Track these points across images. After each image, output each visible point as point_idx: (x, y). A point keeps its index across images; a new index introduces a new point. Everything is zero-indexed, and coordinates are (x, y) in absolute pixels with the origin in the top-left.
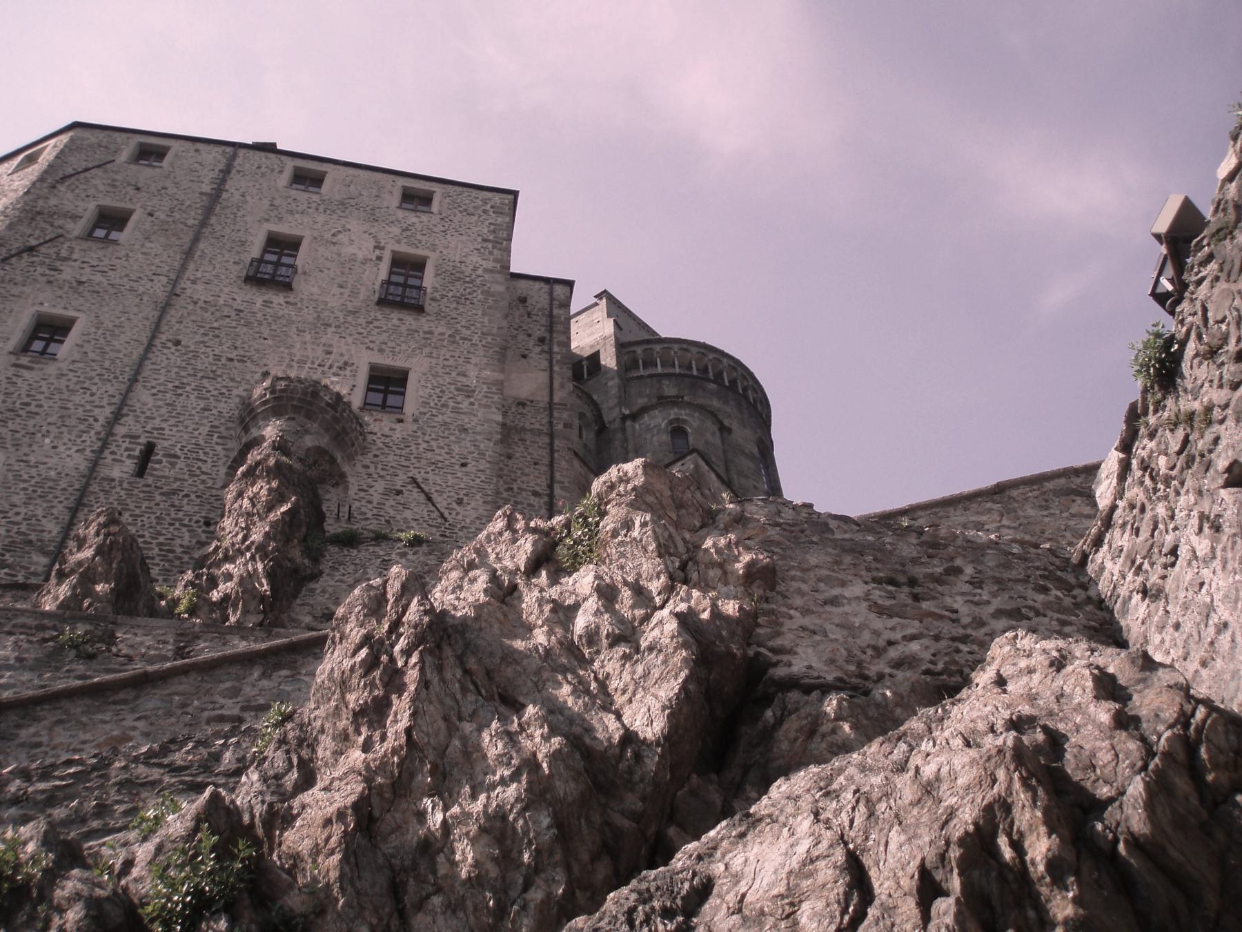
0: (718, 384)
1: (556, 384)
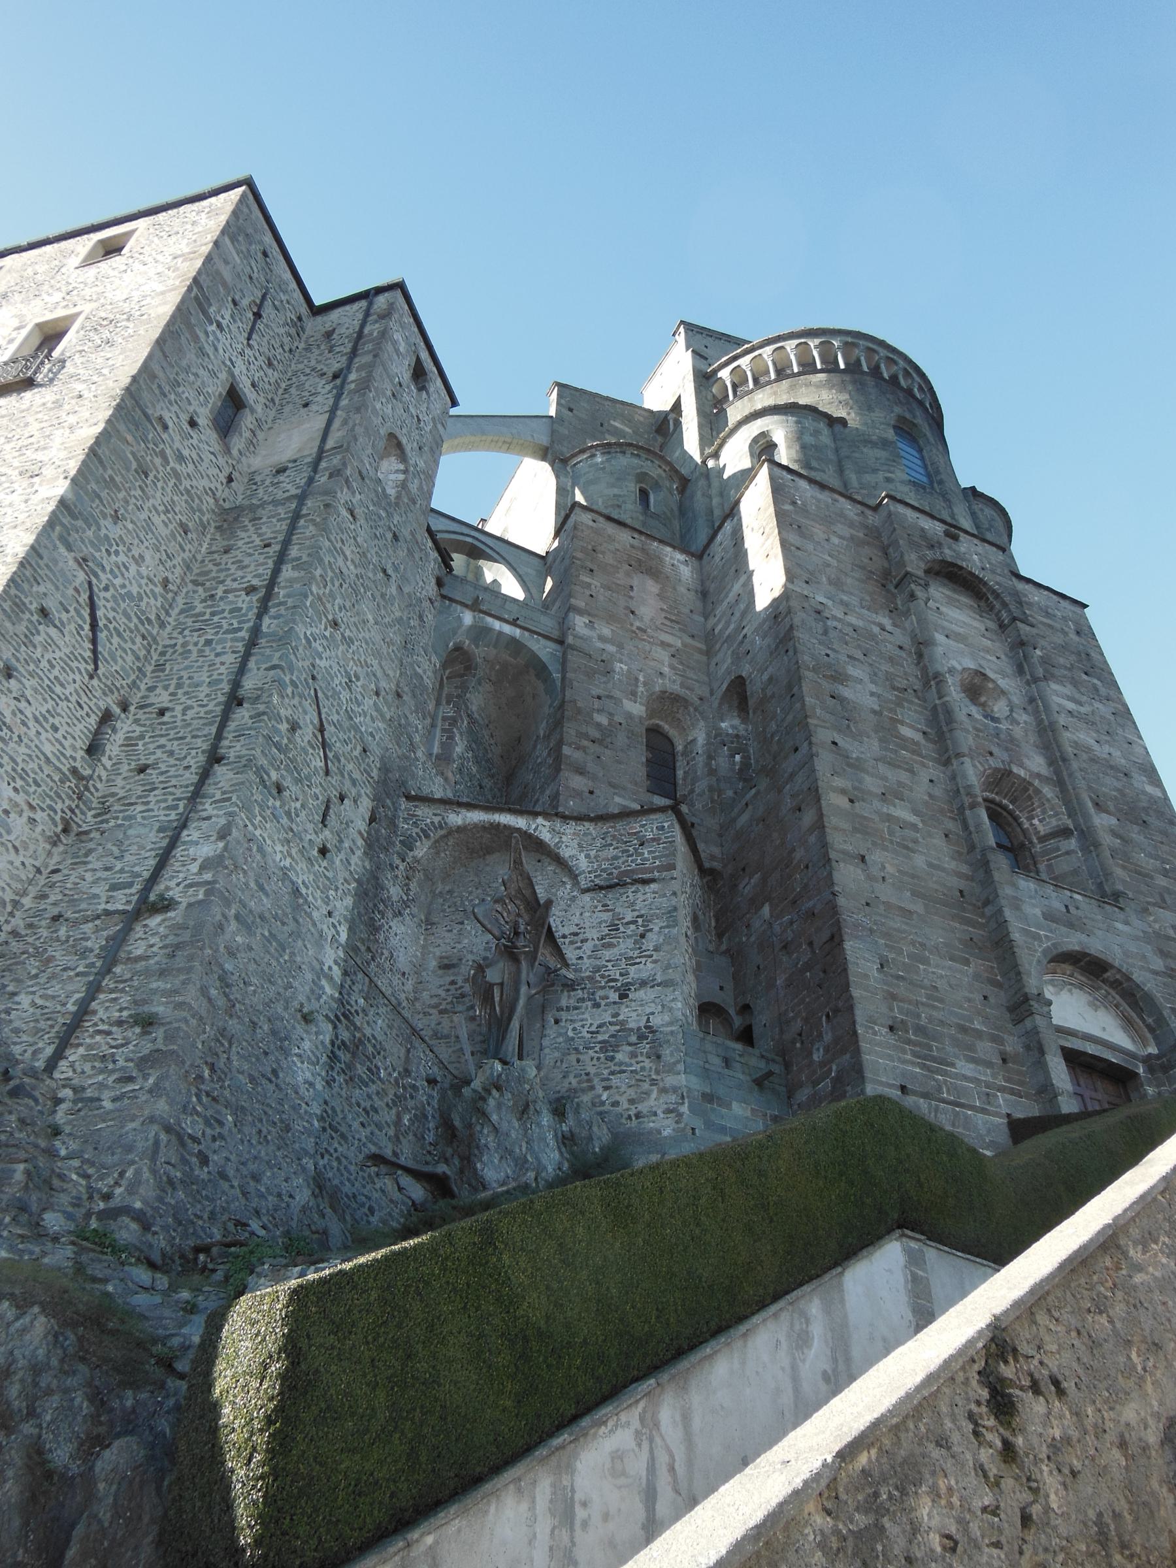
1: (337, 423)
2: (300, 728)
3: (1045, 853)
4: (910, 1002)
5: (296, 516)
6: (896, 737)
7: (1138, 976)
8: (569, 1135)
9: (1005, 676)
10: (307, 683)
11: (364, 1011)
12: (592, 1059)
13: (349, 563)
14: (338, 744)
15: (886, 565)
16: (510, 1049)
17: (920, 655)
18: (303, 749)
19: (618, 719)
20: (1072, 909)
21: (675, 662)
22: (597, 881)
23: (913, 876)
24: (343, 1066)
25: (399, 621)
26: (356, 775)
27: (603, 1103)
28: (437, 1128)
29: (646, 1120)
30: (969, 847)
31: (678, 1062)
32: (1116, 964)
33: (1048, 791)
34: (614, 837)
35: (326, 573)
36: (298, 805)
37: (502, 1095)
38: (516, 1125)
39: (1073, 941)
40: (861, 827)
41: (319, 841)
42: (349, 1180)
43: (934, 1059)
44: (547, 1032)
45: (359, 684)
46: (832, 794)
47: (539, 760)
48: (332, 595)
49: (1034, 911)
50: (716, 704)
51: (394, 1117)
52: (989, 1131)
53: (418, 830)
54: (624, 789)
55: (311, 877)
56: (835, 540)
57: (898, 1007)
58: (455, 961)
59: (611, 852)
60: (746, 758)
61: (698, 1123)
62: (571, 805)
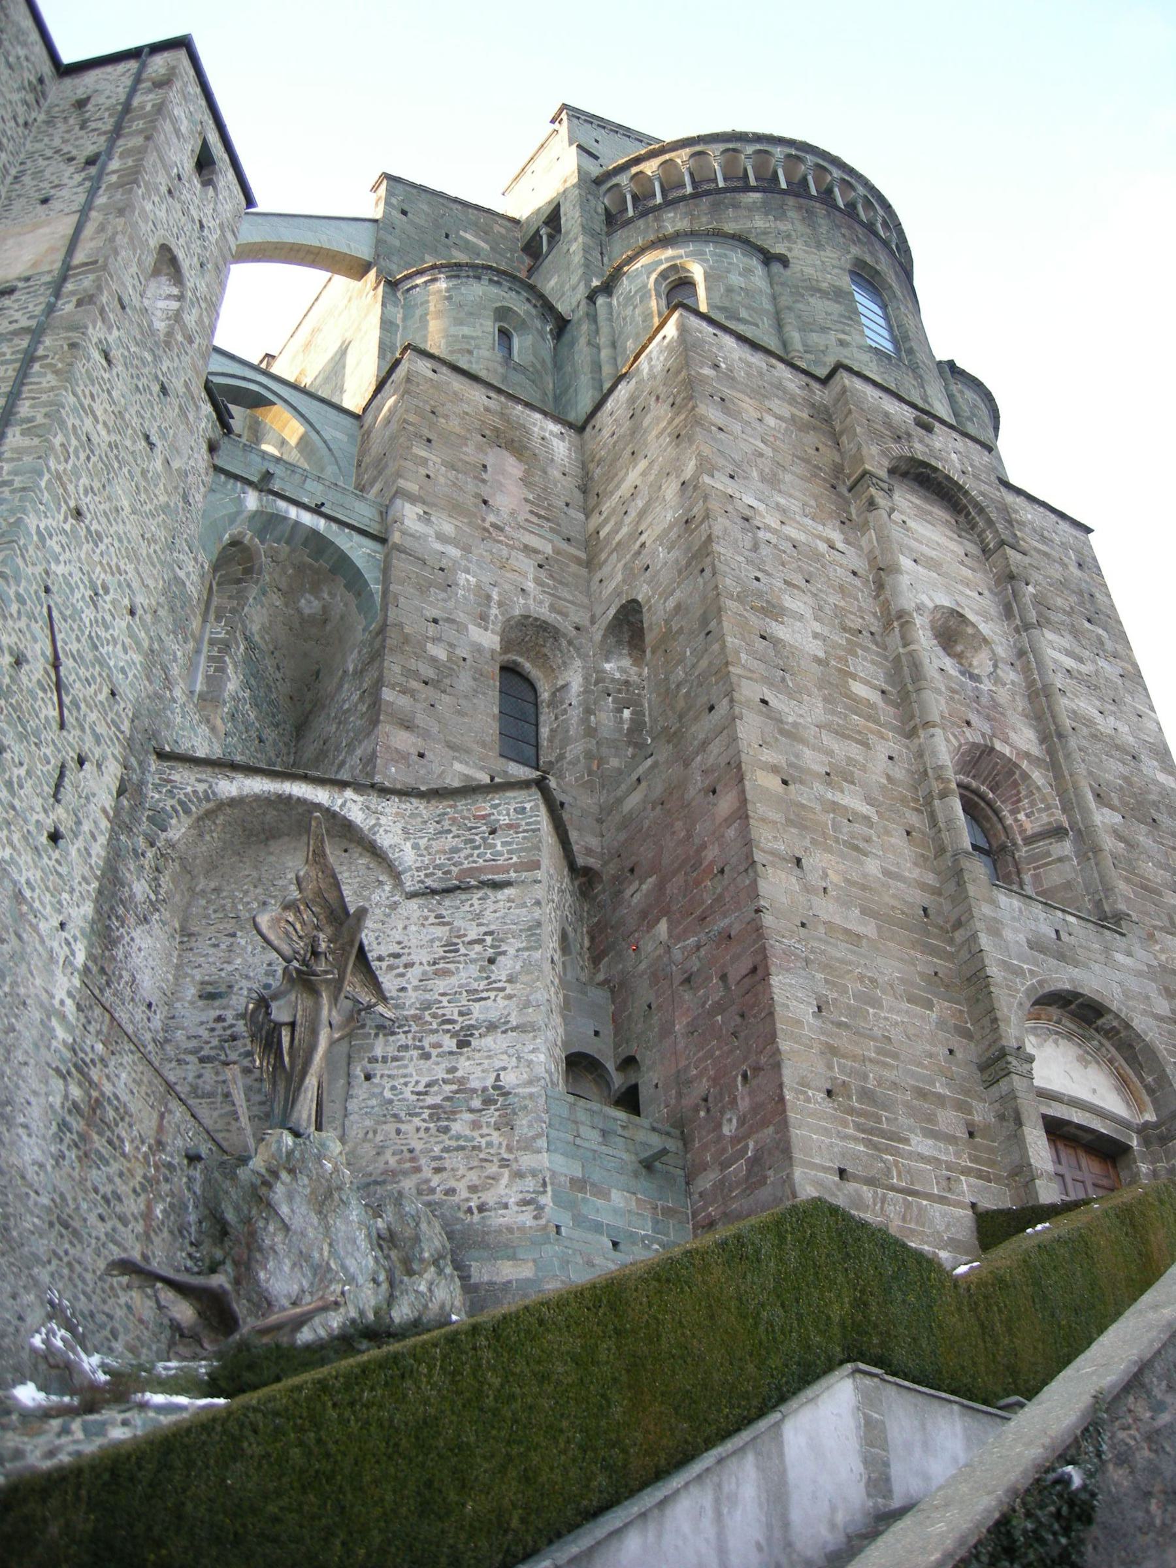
0: (764, 191)
1: (89, 230)
2: (27, 661)
3: (1033, 858)
4: (854, 1058)
5: (29, 358)
6: (847, 696)
7: (1140, 1023)
8: (385, 1233)
9: (987, 618)
10: (38, 598)
11: (102, 1060)
12: (418, 1130)
13: (100, 427)
14: (78, 685)
15: (838, 459)
16: (305, 1116)
17: (880, 586)
18: (30, 691)
19: (462, 652)
20: (1064, 935)
21: (542, 574)
22: (429, 882)
23: (864, 888)
24: (75, 1137)
25: (165, 508)
26: (101, 729)
27: (432, 1191)
28: (200, 1222)
29: (492, 1214)
30: (936, 849)
31: (539, 1136)
32: (1114, 1008)
33: (1038, 776)
34: (454, 820)
35: (69, 441)
36: (22, 772)
37: (295, 1178)
38: (315, 1221)
39: (1064, 978)
40: (798, 819)
41: (49, 823)
42: (84, 1293)
43: (882, 1134)
44: (353, 1092)
45: (107, 598)
46: (759, 772)
47: (346, 706)
48: (76, 472)
49: (1016, 937)
50: (598, 637)
51: (142, 1207)
52: (948, 1225)
53: (174, 802)
54: (468, 751)
55: (39, 874)
56: (771, 421)
57: (839, 1065)
58: (223, 989)
59: (449, 841)
60: (638, 714)
61: (565, 1219)
62: (392, 773)
